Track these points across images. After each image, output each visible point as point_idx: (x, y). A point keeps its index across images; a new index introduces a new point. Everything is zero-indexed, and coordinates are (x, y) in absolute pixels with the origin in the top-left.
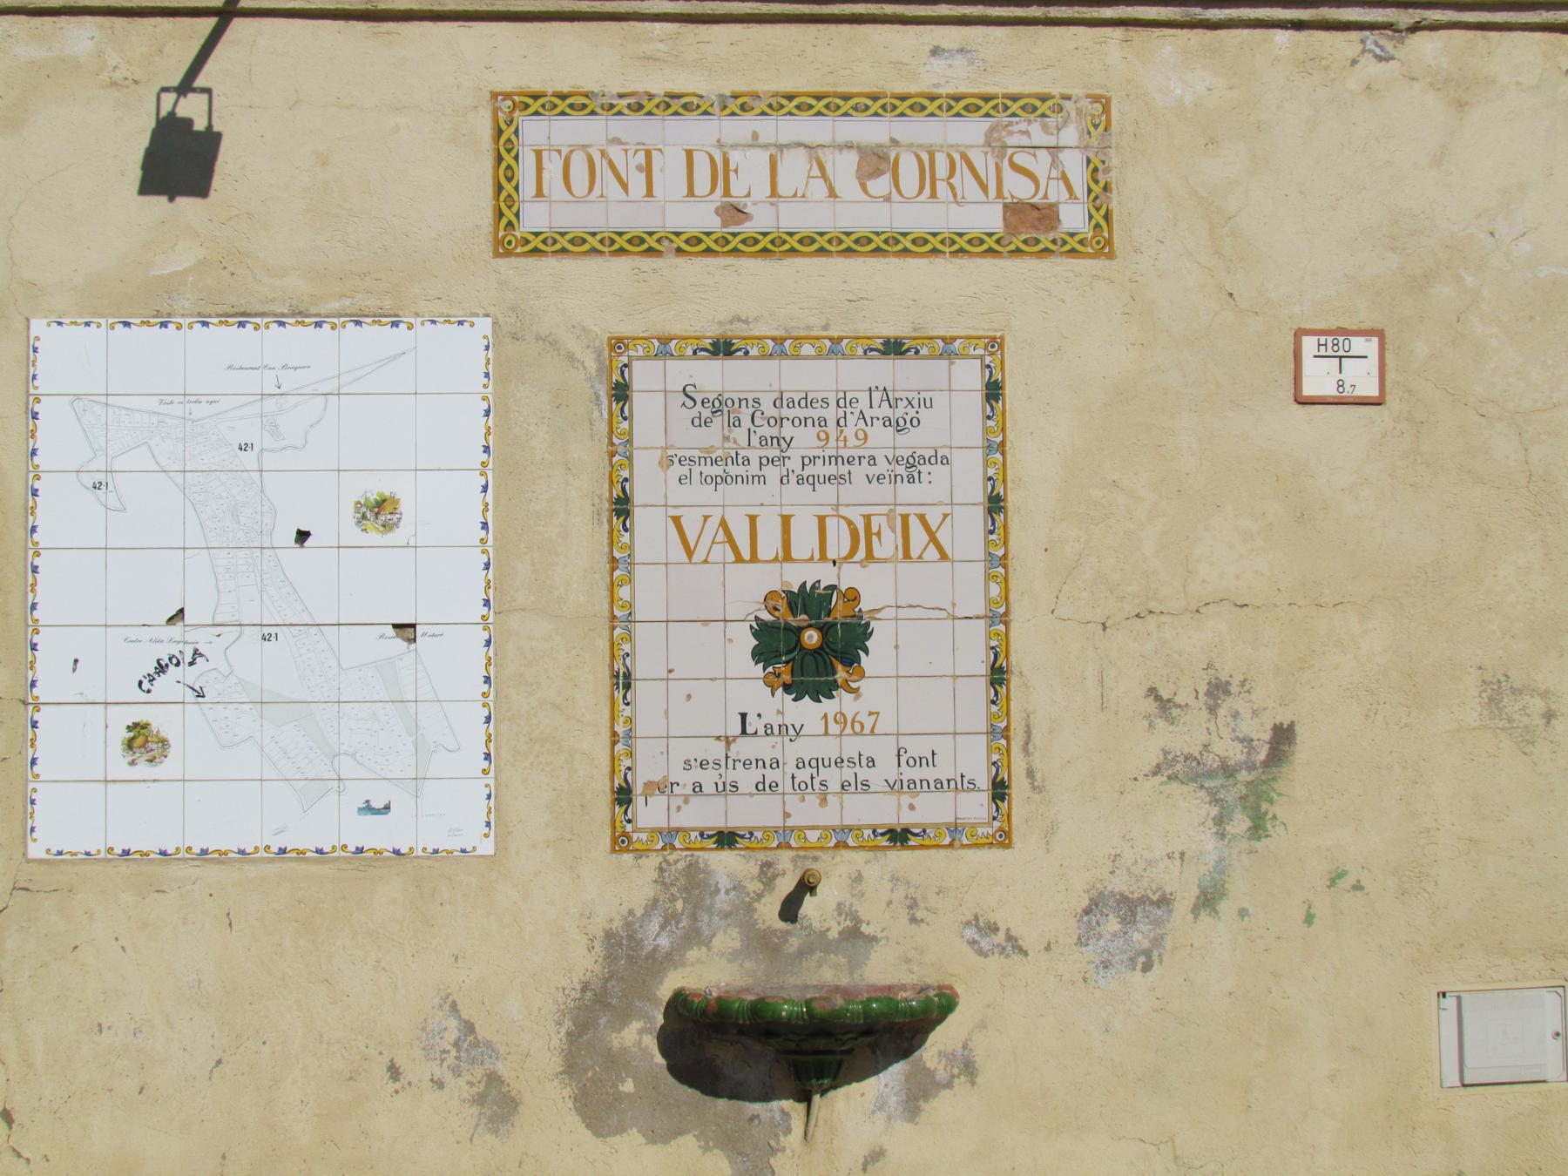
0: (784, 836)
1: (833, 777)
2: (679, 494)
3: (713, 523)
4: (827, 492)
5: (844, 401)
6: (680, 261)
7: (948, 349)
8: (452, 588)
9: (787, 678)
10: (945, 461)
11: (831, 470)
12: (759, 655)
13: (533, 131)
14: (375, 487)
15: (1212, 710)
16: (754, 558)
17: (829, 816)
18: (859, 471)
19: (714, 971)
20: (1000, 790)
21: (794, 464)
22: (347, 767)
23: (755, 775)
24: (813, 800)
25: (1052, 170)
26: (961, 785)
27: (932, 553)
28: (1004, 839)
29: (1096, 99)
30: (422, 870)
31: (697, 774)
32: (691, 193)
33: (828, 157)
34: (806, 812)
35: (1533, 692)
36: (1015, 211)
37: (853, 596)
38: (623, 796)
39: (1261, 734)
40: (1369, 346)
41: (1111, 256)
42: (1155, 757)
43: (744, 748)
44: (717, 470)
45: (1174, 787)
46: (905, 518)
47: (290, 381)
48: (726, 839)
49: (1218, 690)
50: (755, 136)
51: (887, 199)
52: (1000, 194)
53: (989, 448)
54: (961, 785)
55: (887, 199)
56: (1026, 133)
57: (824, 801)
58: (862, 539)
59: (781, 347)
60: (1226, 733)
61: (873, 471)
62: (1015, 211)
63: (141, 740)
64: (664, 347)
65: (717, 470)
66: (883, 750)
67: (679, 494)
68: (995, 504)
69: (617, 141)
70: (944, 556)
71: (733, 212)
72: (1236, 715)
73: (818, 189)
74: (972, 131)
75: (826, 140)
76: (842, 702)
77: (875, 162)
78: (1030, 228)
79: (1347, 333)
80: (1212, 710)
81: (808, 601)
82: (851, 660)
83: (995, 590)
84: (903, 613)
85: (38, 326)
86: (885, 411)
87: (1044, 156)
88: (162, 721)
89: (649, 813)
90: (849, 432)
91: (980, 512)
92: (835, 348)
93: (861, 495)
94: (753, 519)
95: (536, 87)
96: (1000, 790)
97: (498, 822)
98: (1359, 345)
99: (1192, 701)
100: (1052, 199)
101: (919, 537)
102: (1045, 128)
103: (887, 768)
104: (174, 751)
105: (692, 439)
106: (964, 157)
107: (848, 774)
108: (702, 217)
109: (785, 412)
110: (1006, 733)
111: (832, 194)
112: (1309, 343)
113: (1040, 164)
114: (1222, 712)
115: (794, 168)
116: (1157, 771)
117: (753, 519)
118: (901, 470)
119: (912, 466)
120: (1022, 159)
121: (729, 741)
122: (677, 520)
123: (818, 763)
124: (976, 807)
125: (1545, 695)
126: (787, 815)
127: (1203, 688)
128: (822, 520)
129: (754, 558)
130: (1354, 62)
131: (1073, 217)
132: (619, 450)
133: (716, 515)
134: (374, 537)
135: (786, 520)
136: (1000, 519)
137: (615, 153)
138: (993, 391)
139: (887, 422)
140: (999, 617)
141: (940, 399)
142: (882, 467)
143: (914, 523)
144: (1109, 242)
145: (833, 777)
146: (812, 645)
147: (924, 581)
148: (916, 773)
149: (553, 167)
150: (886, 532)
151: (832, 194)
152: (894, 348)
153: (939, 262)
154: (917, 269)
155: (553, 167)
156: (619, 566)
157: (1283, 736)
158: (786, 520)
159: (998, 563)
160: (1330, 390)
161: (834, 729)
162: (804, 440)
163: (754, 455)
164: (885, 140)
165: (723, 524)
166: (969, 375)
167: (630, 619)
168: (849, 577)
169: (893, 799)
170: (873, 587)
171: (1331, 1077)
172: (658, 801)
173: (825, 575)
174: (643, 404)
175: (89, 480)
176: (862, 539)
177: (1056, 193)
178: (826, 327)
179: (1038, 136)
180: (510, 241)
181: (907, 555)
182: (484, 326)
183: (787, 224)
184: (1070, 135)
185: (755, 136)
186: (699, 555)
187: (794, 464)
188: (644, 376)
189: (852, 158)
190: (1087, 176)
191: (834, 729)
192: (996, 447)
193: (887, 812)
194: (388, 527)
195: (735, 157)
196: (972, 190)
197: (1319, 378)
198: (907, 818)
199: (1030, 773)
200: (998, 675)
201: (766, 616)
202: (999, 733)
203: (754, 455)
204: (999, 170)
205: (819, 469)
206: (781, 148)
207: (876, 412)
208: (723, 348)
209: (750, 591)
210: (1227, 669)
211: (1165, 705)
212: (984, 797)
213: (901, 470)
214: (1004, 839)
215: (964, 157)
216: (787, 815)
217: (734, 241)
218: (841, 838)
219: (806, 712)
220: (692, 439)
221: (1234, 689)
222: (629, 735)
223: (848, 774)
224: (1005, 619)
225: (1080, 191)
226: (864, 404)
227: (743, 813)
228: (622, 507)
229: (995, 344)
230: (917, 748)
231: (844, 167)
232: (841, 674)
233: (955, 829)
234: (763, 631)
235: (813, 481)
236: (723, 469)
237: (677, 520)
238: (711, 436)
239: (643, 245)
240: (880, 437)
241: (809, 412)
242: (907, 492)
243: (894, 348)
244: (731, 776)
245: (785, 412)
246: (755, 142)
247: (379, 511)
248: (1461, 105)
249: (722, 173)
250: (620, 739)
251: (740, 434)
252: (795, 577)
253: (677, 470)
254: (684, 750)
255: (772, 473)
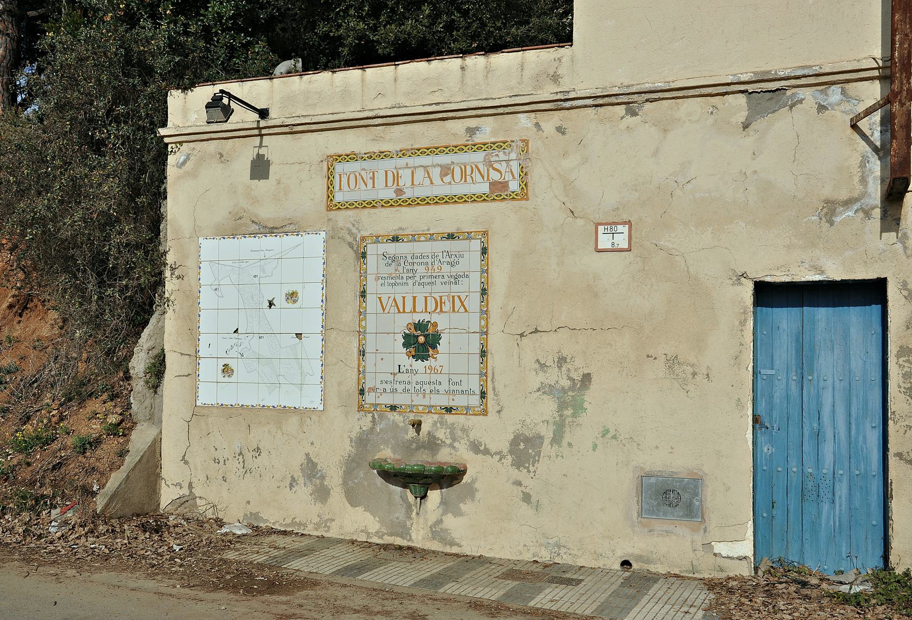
0: (411, 408)
1: (427, 388)
2: (381, 290)
3: (391, 299)
4: (428, 288)
5: (434, 256)
6: (382, 209)
7: (469, 236)
8: (313, 322)
9: (413, 353)
10: (467, 276)
11: (429, 280)
12: (404, 345)
13: (339, 168)
14: (291, 289)
15: (560, 367)
16: (404, 312)
17: (426, 402)
18: (439, 281)
19: (388, 454)
20: (483, 395)
21: (417, 279)
22: (282, 380)
23: (403, 386)
24: (421, 396)
25: (507, 169)
26: (470, 393)
27: (462, 309)
28: (485, 413)
29: (523, 141)
30: (302, 413)
31: (384, 386)
32: (386, 186)
33: (430, 169)
34: (418, 400)
35: (688, 364)
36: (493, 185)
37: (435, 325)
38: (362, 392)
39: (577, 376)
40: (624, 229)
41: (527, 199)
42: (538, 385)
43: (399, 377)
44: (393, 281)
45: (545, 397)
46: (453, 297)
47: (268, 254)
48: (393, 408)
49: (562, 360)
50: (407, 164)
51: (450, 183)
52: (488, 179)
53: (482, 272)
54: (470, 393)
55: (450, 183)
56: (497, 155)
57: (424, 397)
58: (439, 304)
59: (414, 238)
60: (565, 377)
61: (444, 280)
62: (493, 185)
63: (227, 370)
64: (377, 239)
65: (393, 281)
66: (444, 379)
67: (381, 290)
68: (484, 292)
69: (364, 169)
70: (466, 311)
71: (399, 191)
72: (569, 370)
73: (427, 181)
74: (479, 157)
75: (430, 163)
76: (431, 362)
77: (446, 170)
78: (498, 191)
79: (616, 224)
80: (560, 367)
81: (420, 326)
82: (434, 347)
83: (483, 323)
84: (452, 331)
85: (201, 240)
86: (448, 259)
87: (504, 164)
88: (233, 364)
89: (370, 398)
90: (435, 267)
91: (479, 294)
92: (431, 238)
93: (439, 289)
94: (404, 298)
95: (340, 152)
96: (483, 395)
97: (324, 400)
98: (620, 228)
99: (552, 364)
100: (507, 179)
101: (458, 304)
102: (505, 153)
103: (445, 386)
104: (235, 373)
105: (385, 271)
106: (476, 166)
107: (432, 387)
108: (390, 194)
109: (415, 260)
110: (486, 374)
111: (432, 183)
112: (601, 229)
113: (503, 167)
114: (564, 369)
115: (420, 174)
116: (539, 390)
117: (404, 298)
118: (452, 280)
119: (456, 279)
120: (496, 166)
121: (395, 374)
122: (380, 298)
123: (423, 383)
124: (475, 400)
125: (693, 366)
126: (412, 401)
127: (556, 360)
128: (426, 298)
129: (404, 312)
130: (622, 118)
131: (514, 186)
132: (363, 275)
133: (392, 296)
134: (291, 305)
135: (414, 298)
136: (485, 297)
137: (363, 173)
138: (484, 251)
139: (448, 263)
140: (485, 333)
141: (466, 254)
142: (446, 279)
143: (456, 299)
144: (526, 194)
145: (427, 388)
146: (422, 342)
147: (459, 319)
148: (455, 388)
149: (345, 180)
150: (447, 302)
151: (432, 183)
152: (451, 237)
153: (467, 205)
154: (460, 207)
155: (345, 180)
156: (362, 314)
157: (587, 378)
158: (414, 298)
159: (485, 313)
160: (609, 246)
161: (428, 371)
162: (421, 270)
163: (405, 276)
164: (449, 162)
165: (394, 300)
166: (476, 245)
167: (365, 332)
168: (435, 318)
169: (447, 396)
170: (442, 322)
171: (602, 510)
172: (373, 394)
173: (426, 317)
174: (371, 260)
175: (214, 287)
176: (439, 304)
177: (508, 177)
178: (428, 230)
179: (502, 156)
180: (332, 206)
181: (454, 310)
182: (323, 234)
183: (417, 195)
184: (513, 156)
185: (407, 164)
186: (386, 311)
187: (417, 279)
188: (371, 249)
189: (438, 170)
190: (519, 170)
191: (428, 371)
192: (485, 271)
193: (445, 401)
194: (295, 302)
195: (401, 172)
196: (478, 178)
197: (605, 241)
198: (452, 404)
199: (494, 389)
200: (483, 354)
201: (407, 332)
202: (483, 375)
203: (405, 276)
204: (488, 170)
205: (426, 280)
206: (415, 168)
207: (444, 260)
208: (395, 239)
209: (403, 323)
210: (565, 353)
211: (543, 366)
212: (478, 397)
213: (452, 280)
214: (485, 413)
215: (476, 166)
216: (412, 401)
217: (400, 202)
218: (430, 409)
219: (419, 365)
220: (385, 271)
221: (568, 361)
222: (364, 372)
223: (432, 387)
224: (486, 333)
225: (517, 176)
226: (440, 257)
227: (398, 400)
228: (363, 294)
229: (485, 233)
230: (455, 379)
231: (436, 173)
232: (431, 352)
233: (467, 408)
234: (406, 336)
235: (423, 284)
236: (394, 280)
237: (380, 298)
238: (391, 269)
239: (371, 205)
240: (446, 268)
241: (423, 260)
242: (455, 288)
243: (451, 237)
244: (395, 386)
245: (415, 260)
246: (407, 166)
247: (292, 296)
248: (665, 131)
249: (396, 178)
250: (361, 372)
251: (400, 268)
252: (417, 318)
253: (380, 281)
254: (381, 377)
255: (410, 282)
